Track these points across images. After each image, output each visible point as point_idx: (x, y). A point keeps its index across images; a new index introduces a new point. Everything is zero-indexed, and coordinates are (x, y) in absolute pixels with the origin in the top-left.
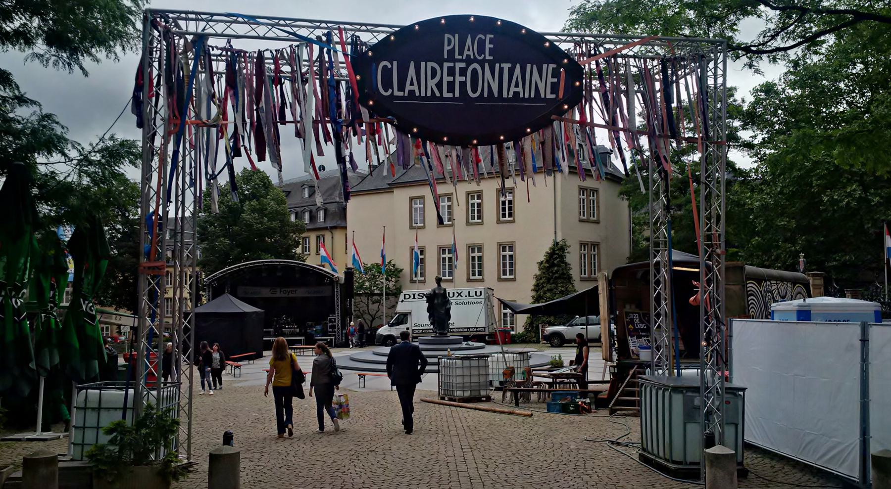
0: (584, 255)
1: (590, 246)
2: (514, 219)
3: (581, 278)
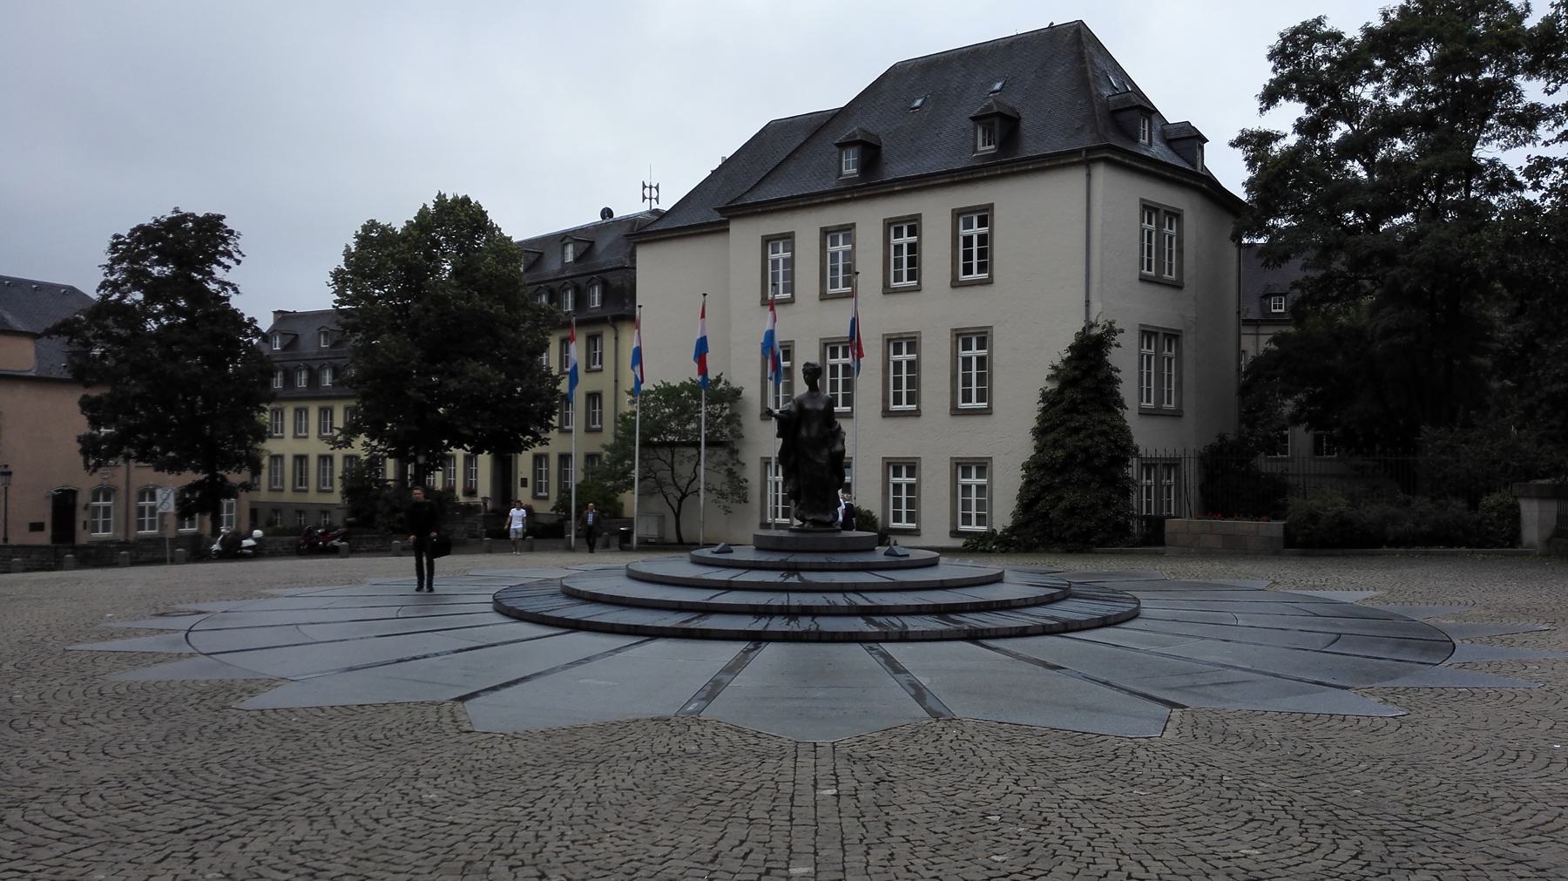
0: (1149, 358)
1: (1161, 335)
2: (991, 276)
3: (1140, 408)
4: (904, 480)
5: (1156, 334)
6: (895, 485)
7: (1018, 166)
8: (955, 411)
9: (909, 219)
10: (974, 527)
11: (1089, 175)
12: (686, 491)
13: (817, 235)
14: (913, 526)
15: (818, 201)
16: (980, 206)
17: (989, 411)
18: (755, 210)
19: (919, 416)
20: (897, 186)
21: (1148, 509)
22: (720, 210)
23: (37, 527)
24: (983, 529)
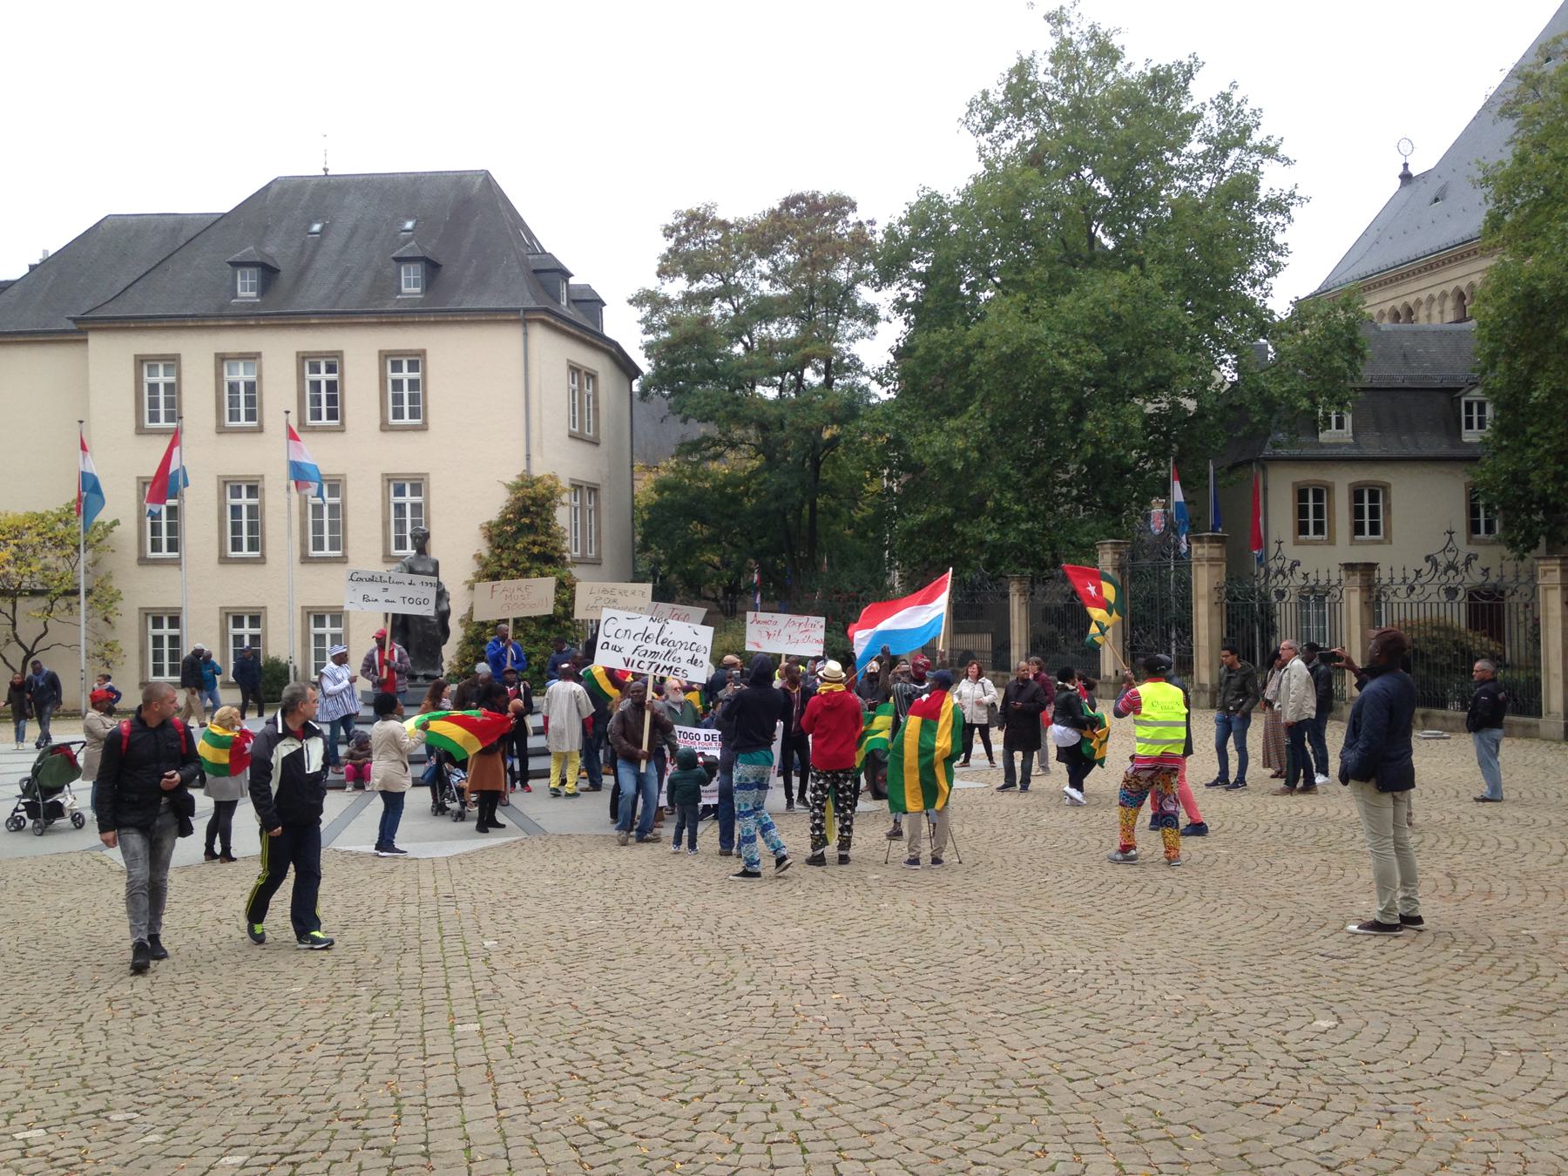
5: (581, 487)
11: (526, 334)
13: (211, 361)
22: (75, 320)
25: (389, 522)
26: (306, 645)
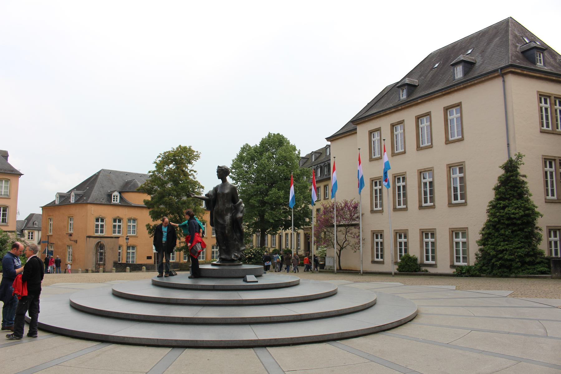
3: (546, 199)
4: (430, 240)
6: (426, 242)
7: (470, 82)
8: (450, 205)
9: (426, 114)
10: (461, 263)
12: (343, 247)
13: (389, 127)
14: (433, 262)
15: (388, 112)
16: (455, 104)
17: (466, 204)
18: (365, 120)
19: (435, 208)
20: (419, 100)
21: (556, 253)
23: (149, 258)
24: (466, 264)
25: (450, 188)
26: (422, 246)
